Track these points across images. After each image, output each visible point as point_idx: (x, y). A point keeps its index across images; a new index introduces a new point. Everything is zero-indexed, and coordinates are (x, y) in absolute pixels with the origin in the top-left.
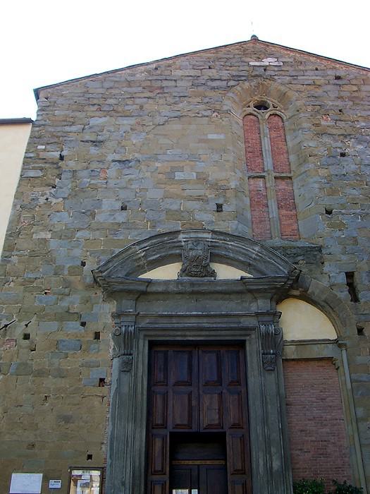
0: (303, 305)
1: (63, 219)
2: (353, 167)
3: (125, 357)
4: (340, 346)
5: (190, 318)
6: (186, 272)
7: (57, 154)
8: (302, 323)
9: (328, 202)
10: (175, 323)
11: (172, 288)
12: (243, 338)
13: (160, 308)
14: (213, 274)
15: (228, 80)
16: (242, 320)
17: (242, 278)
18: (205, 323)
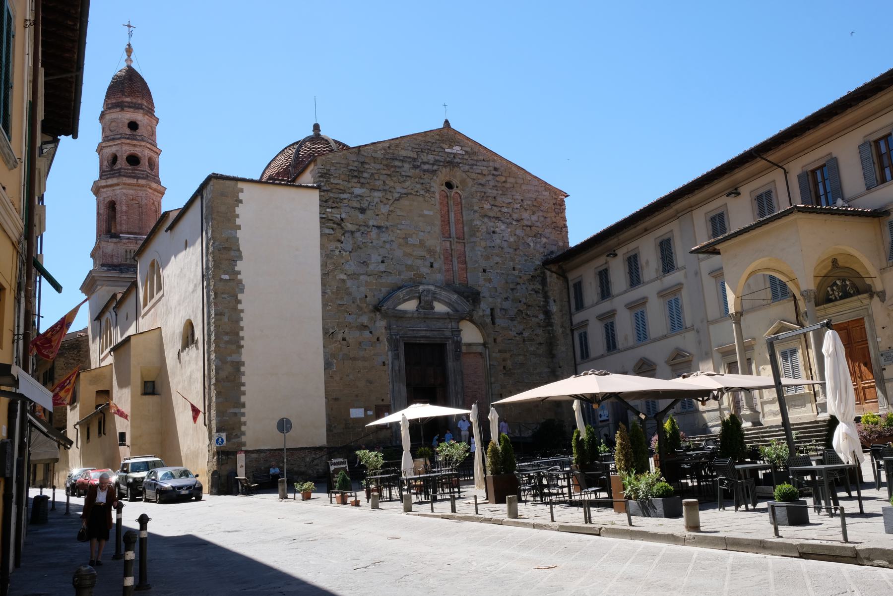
0: (469, 323)
1: (352, 267)
2: (498, 241)
4: (486, 347)
5: (422, 331)
7: (338, 216)
8: (470, 334)
9: (484, 263)
14: (433, 308)
15: (433, 165)
18: (428, 334)
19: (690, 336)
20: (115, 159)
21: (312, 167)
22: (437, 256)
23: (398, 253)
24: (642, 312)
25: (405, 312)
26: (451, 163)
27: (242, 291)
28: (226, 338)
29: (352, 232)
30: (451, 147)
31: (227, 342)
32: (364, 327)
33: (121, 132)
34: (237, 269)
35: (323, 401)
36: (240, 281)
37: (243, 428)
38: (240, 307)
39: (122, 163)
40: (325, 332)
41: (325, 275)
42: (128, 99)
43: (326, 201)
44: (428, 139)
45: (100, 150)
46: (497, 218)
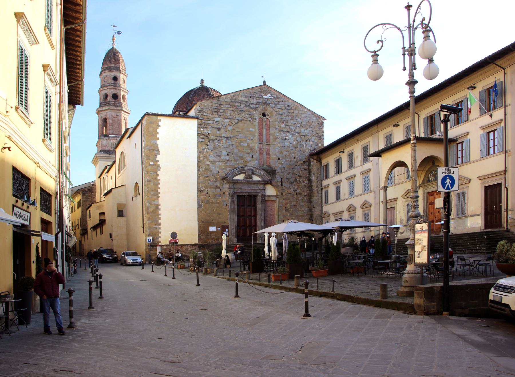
1: (212, 158)
5: (246, 189)
7: (207, 132)
8: (271, 191)
9: (279, 155)
13: (238, 186)
14: (251, 178)
19: (372, 194)
20: (106, 96)
21: (195, 107)
22: (255, 152)
23: (236, 151)
24: (353, 182)
25: (238, 180)
26: (265, 103)
27: (159, 170)
28: (152, 193)
29: (213, 140)
30: (266, 95)
31: (153, 195)
32: (217, 187)
33: (109, 82)
34: (157, 159)
35: (196, 223)
36: (159, 165)
37: (160, 235)
38: (158, 178)
39: (110, 98)
40: (199, 189)
41: (199, 162)
42: (113, 65)
43: (201, 125)
44: (254, 91)
45: (100, 91)
46: (287, 132)
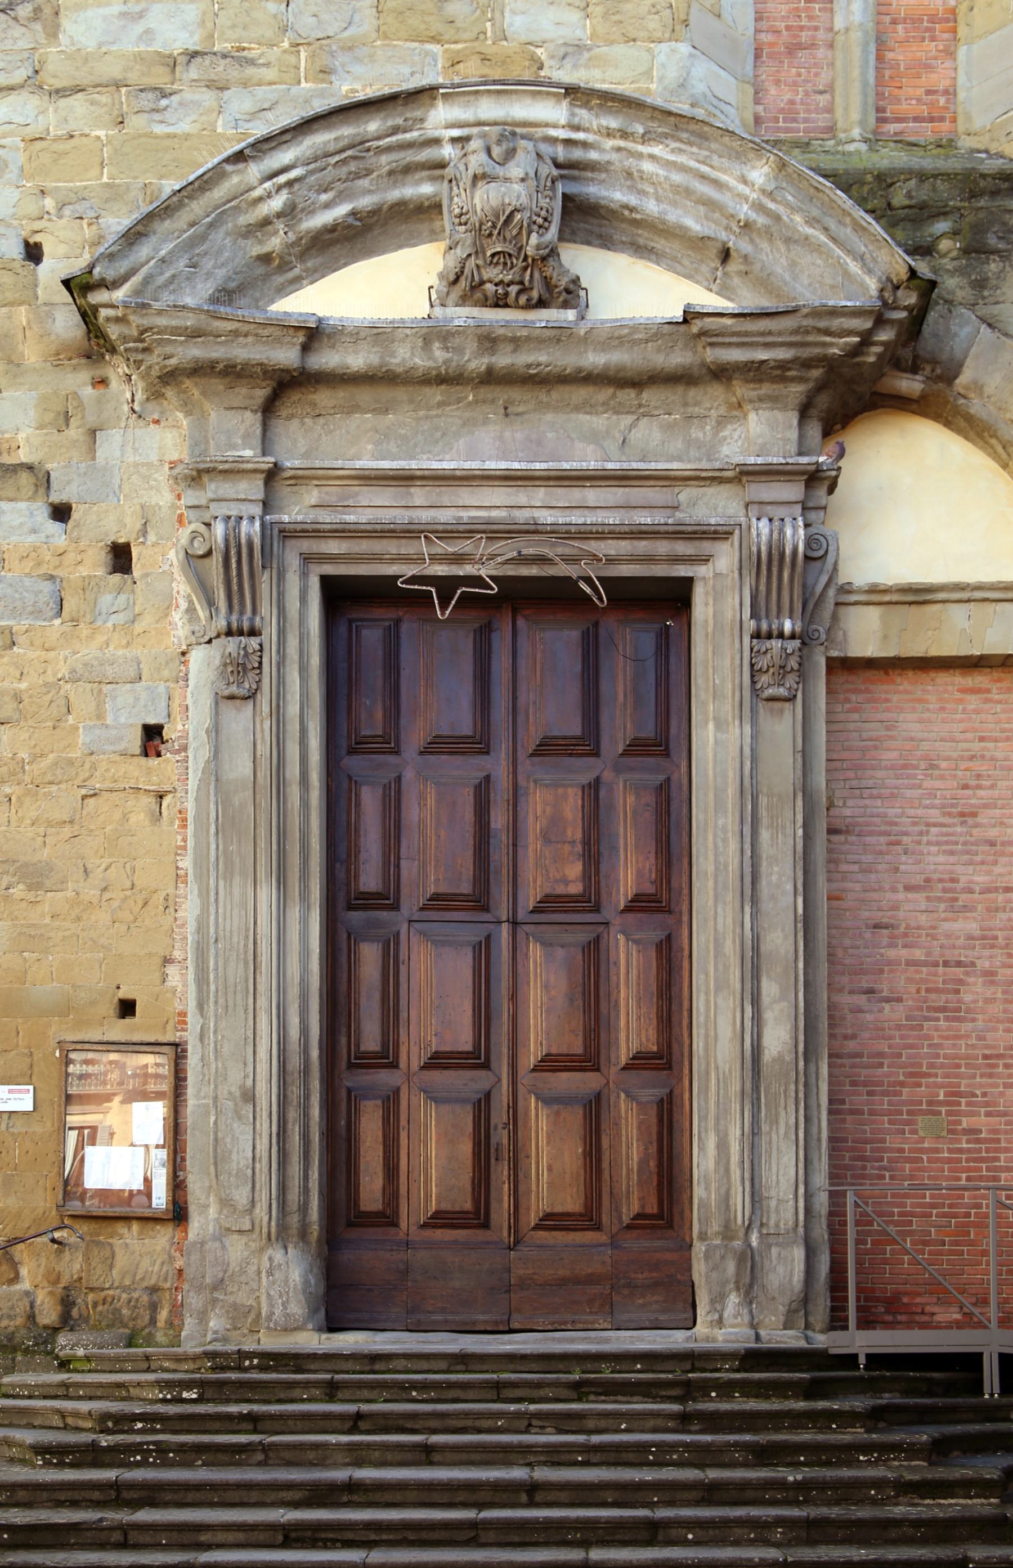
3: (232, 645)
6: (463, 283)
10: (422, 506)
11: (405, 356)
12: (682, 571)
14: (571, 294)
16: (685, 495)
17: (690, 316)
18: (542, 506)
